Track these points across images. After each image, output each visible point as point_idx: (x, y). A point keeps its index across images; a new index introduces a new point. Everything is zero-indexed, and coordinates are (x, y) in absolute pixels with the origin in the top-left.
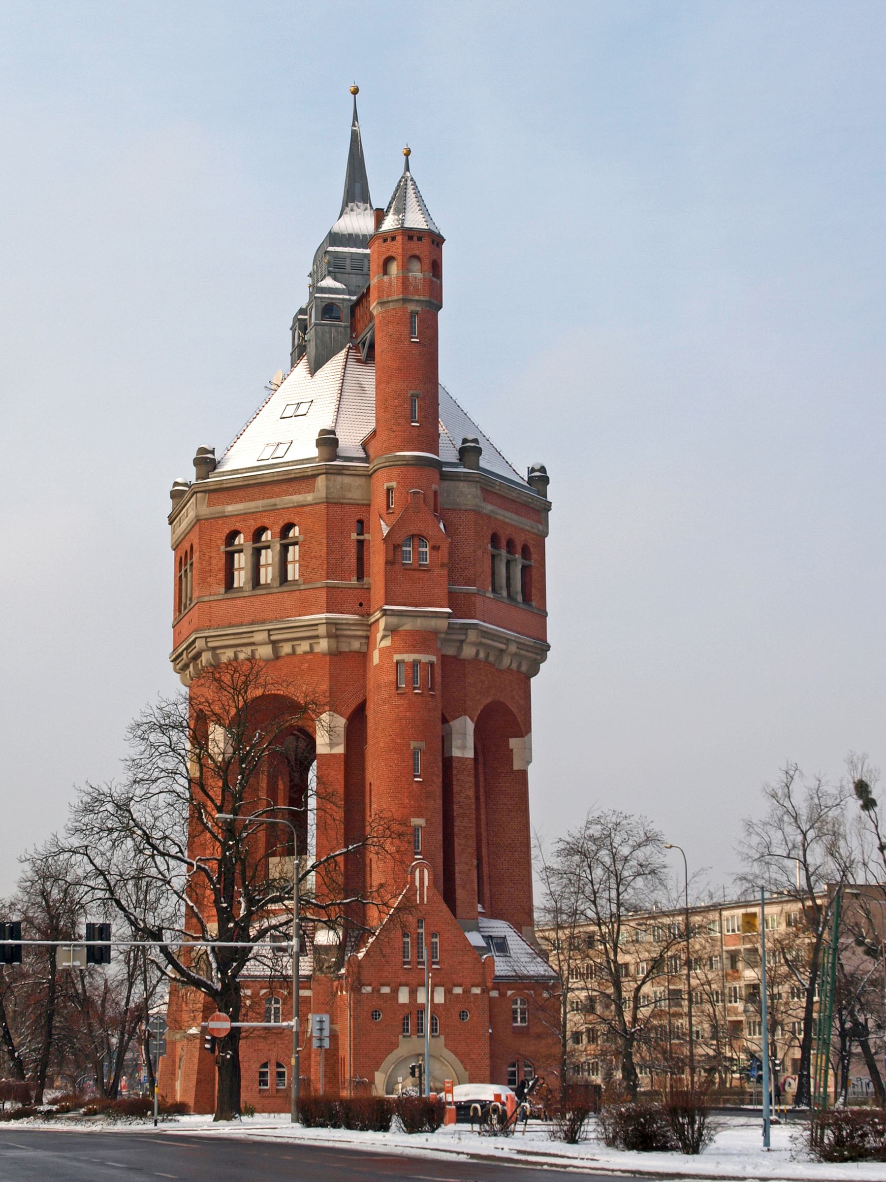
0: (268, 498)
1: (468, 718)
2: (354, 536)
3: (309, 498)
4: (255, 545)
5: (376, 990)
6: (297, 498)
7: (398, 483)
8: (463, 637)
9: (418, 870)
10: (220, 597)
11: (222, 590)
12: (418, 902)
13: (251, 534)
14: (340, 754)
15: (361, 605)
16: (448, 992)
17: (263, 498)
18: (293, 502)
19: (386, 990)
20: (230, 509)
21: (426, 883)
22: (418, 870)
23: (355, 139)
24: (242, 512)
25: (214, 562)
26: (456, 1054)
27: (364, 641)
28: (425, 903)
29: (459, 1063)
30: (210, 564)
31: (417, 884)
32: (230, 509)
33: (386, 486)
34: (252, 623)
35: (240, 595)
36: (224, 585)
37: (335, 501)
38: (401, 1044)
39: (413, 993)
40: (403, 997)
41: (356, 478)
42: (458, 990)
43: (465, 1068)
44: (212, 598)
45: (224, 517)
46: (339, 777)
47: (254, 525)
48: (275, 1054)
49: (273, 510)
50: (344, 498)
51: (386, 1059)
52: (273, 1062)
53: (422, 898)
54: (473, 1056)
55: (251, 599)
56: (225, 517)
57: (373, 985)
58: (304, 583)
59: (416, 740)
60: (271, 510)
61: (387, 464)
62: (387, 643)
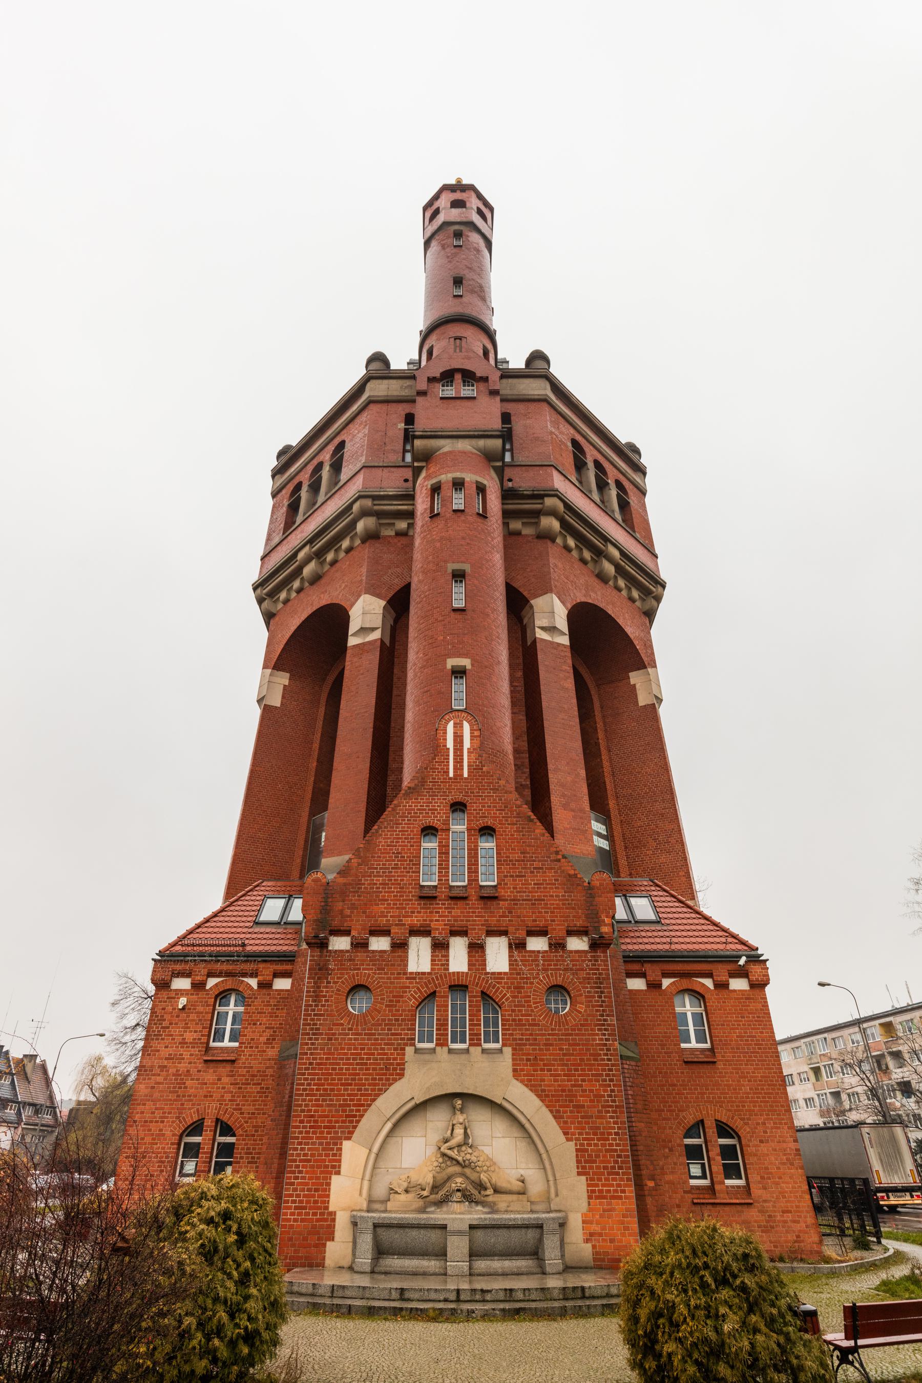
1: (554, 595)
2: (402, 426)
5: (360, 945)
8: (539, 506)
12: (451, 775)
16: (518, 946)
21: (467, 744)
28: (466, 775)
29: (549, 1116)
31: (450, 744)
38: (410, 1069)
39: (440, 947)
42: (537, 944)
43: (565, 1134)
51: (373, 1107)
57: (353, 933)
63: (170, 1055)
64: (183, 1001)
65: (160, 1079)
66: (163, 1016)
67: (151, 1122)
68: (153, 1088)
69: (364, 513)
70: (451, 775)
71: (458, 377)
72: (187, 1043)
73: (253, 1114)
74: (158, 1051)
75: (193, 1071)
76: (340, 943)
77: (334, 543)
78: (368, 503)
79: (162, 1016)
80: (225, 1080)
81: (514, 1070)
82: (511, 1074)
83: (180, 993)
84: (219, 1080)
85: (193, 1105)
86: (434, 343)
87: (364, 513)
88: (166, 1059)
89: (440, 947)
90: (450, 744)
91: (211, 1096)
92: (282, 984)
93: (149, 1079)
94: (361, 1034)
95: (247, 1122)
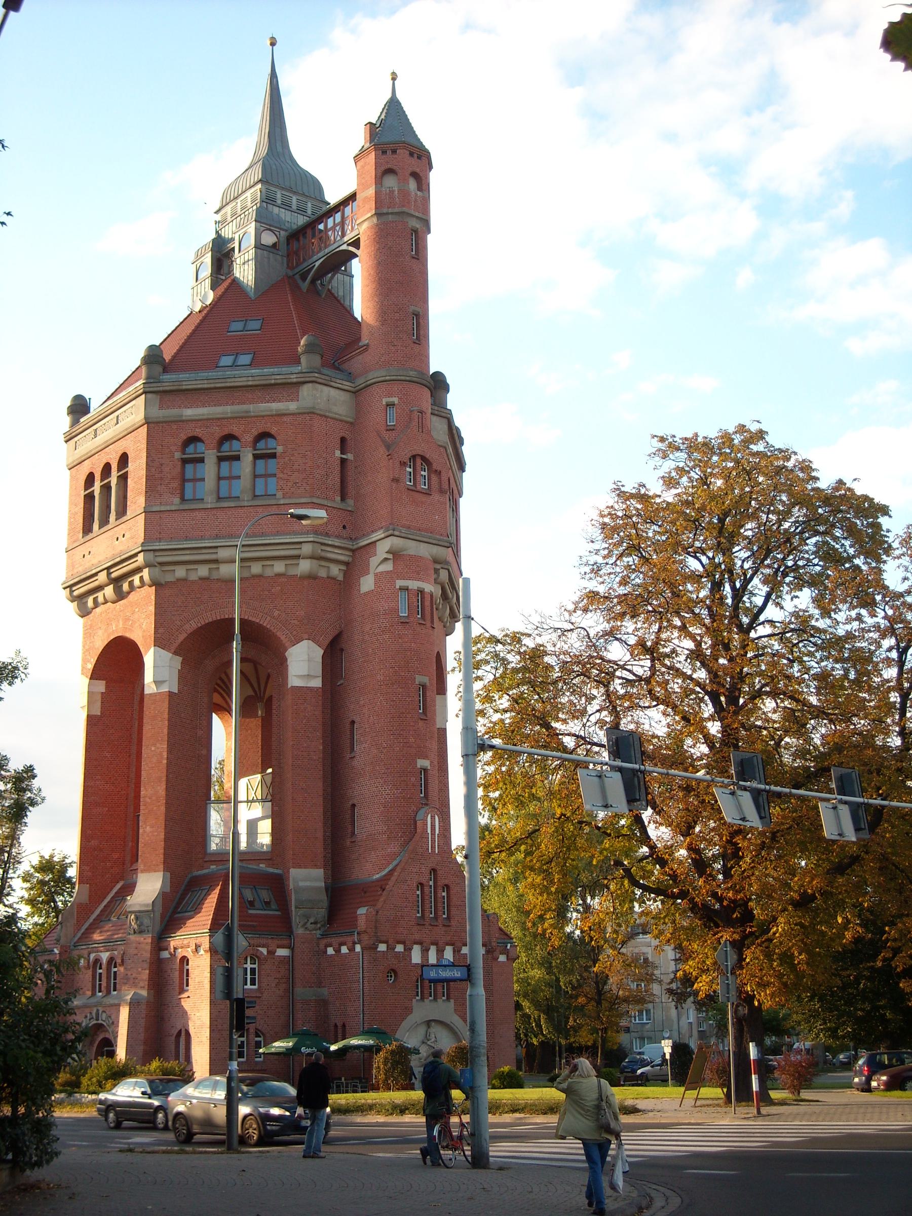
0: (238, 404)
2: (338, 453)
3: (292, 406)
4: (219, 454)
5: (391, 948)
6: (275, 406)
7: (400, 399)
9: (429, 816)
10: (173, 508)
11: (177, 500)
13: (215, 441)
14: (318, 688)
15: (344, 527)
17: (233, 404)
18: (272, 410)
19: (400, 948)
20: (189, 413)
21: (437, 832)
22: (429, 816)
23: (273, 76)
24: (205, 417)
27: (344, 568)
30: (161, 472)
31: (429, 831)
32: (189, 413)
33: (384, 402)
34: (217, 537)
35: (201, 506)
36: (179, 495)
37: (321, 413)
39: (425, 951)
40: (416, 957)
41: (342, 393)
44: (163, 508)
45: (180, 422)
47: (218, 432)
49: (243, 418)
50: (329, 412)
53: (433, 847)
55: (214, 512)
56: (181, 421)
60: (242, 417)
61: (388, 378)
62: (388, 567)
76: (382, 947)
78: (319, 548)
86: (395, 400)
89: (425, 951)
90: (429, 831)
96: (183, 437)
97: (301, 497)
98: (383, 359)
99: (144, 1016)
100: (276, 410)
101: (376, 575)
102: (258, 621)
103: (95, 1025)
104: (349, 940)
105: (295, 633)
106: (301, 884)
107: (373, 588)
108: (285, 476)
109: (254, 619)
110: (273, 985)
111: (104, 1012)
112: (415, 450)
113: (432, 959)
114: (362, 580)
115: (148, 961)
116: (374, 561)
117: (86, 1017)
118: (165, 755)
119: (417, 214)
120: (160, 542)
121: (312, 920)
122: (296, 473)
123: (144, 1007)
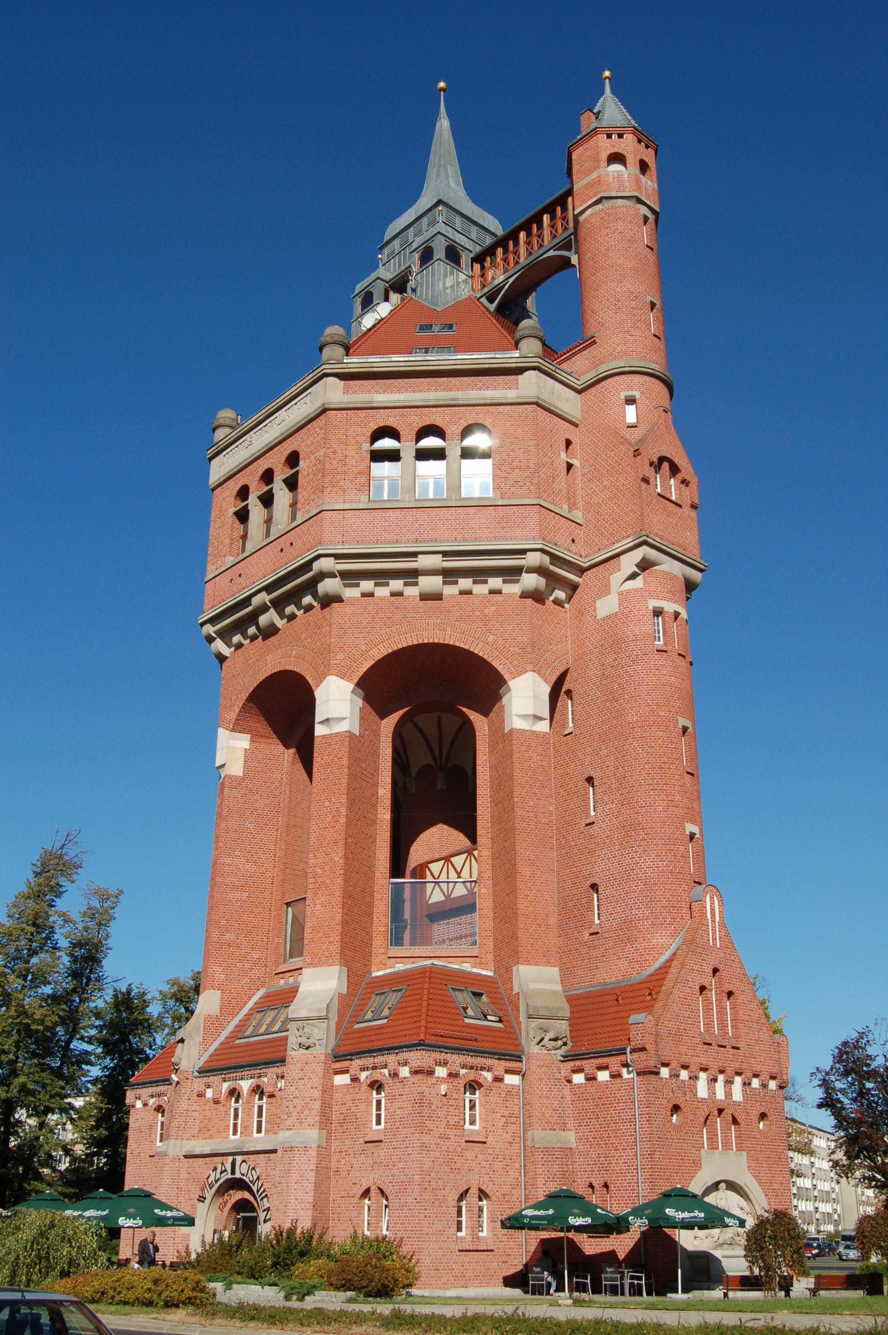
9: (708, 896)
11: (364, 498)
12: (711, 944)
16: (746, 1084)
17: (436, 390)
22: (708, 896)
25: (351, 462)
26: (760, 1183)
28: (718, 946)
32: (381, 398)
42: (755, 1083)
46: (544, 764)
48: (476, 1177)
52: (474, 1191)
53: (714, 939)
54: (776, 1186)
58: (502, 498)
59: (683, 715)
63: (441, 1134)
64: (443, 1089)
65: (437, 1154)
66: (430, 1100)
67: (437, 1189)
68: (433, 1161)
69: (541, 571)
70: (711, 944)
71: (666, 465)
72: (450, 1125)
73: (501, 1185)
74: (432, 1130)
75: (459, 1149)
76: (665, 1072)
77: (480, 574)
78: (547, 559)
79: (430, 1100)
80: (480, 1157)
81: (748, 1167)
82: (747, 1168)
83: (440, 1080)
84: (476, 1157)
85: (462, 1176)
86: (637, 394)
87: (541, 571)
88: (439, 1138)
91: (473, 1170)
92: (512, 1080)
93: (430, 1154)
94: (679, 1139)
95: (497, 1191)
96: (374, 426)
97: (525, 498)
98: (619, 349)
99: (313, 1167)
100: (491, 399)
101: (620, 594)
102: (466, 647)
103: (228, 1180)
104: (614, 1062)
105: (515, 663)
106: (532, 986)
107: (616, 609)
108: (504, 474)
109: (462, 645)
110: (500, 1125)
111: (244, 1161)
112: (663, 451)
113: (720, 1095)
114: (599, 603)
115: (320, 1088)
116: (616, 579)
117: (215, 1169)
118: (343, 810)
119: (648, 203)
120: (343, 545)
121: (551, 1035)
122: (517, 471)
123: (313, 1153)
